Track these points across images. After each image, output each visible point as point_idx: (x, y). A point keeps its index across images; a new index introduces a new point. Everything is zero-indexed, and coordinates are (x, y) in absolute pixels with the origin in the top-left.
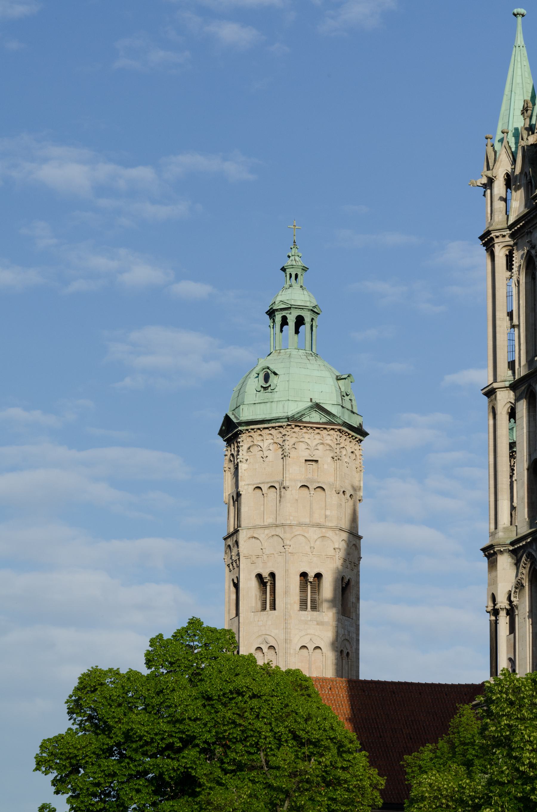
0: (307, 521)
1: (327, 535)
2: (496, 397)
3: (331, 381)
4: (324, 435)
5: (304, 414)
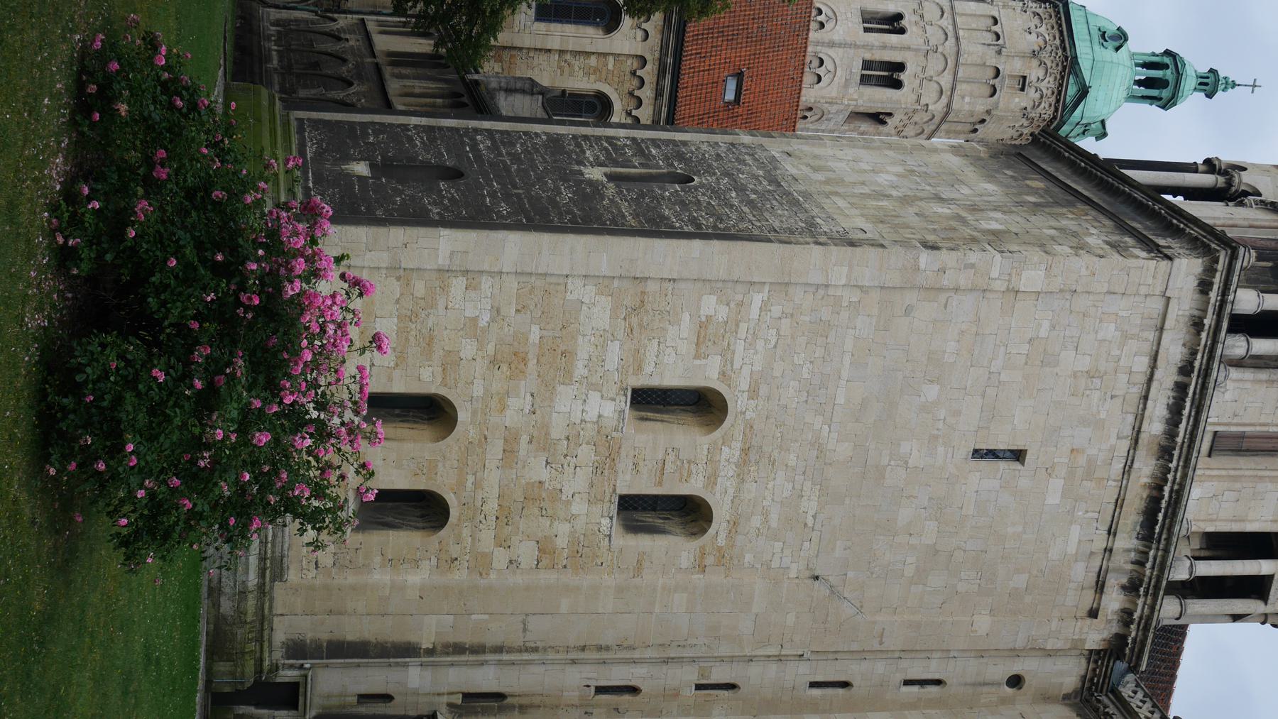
0: (960, 74)
1: (943, 97)
4: (1051, 100)
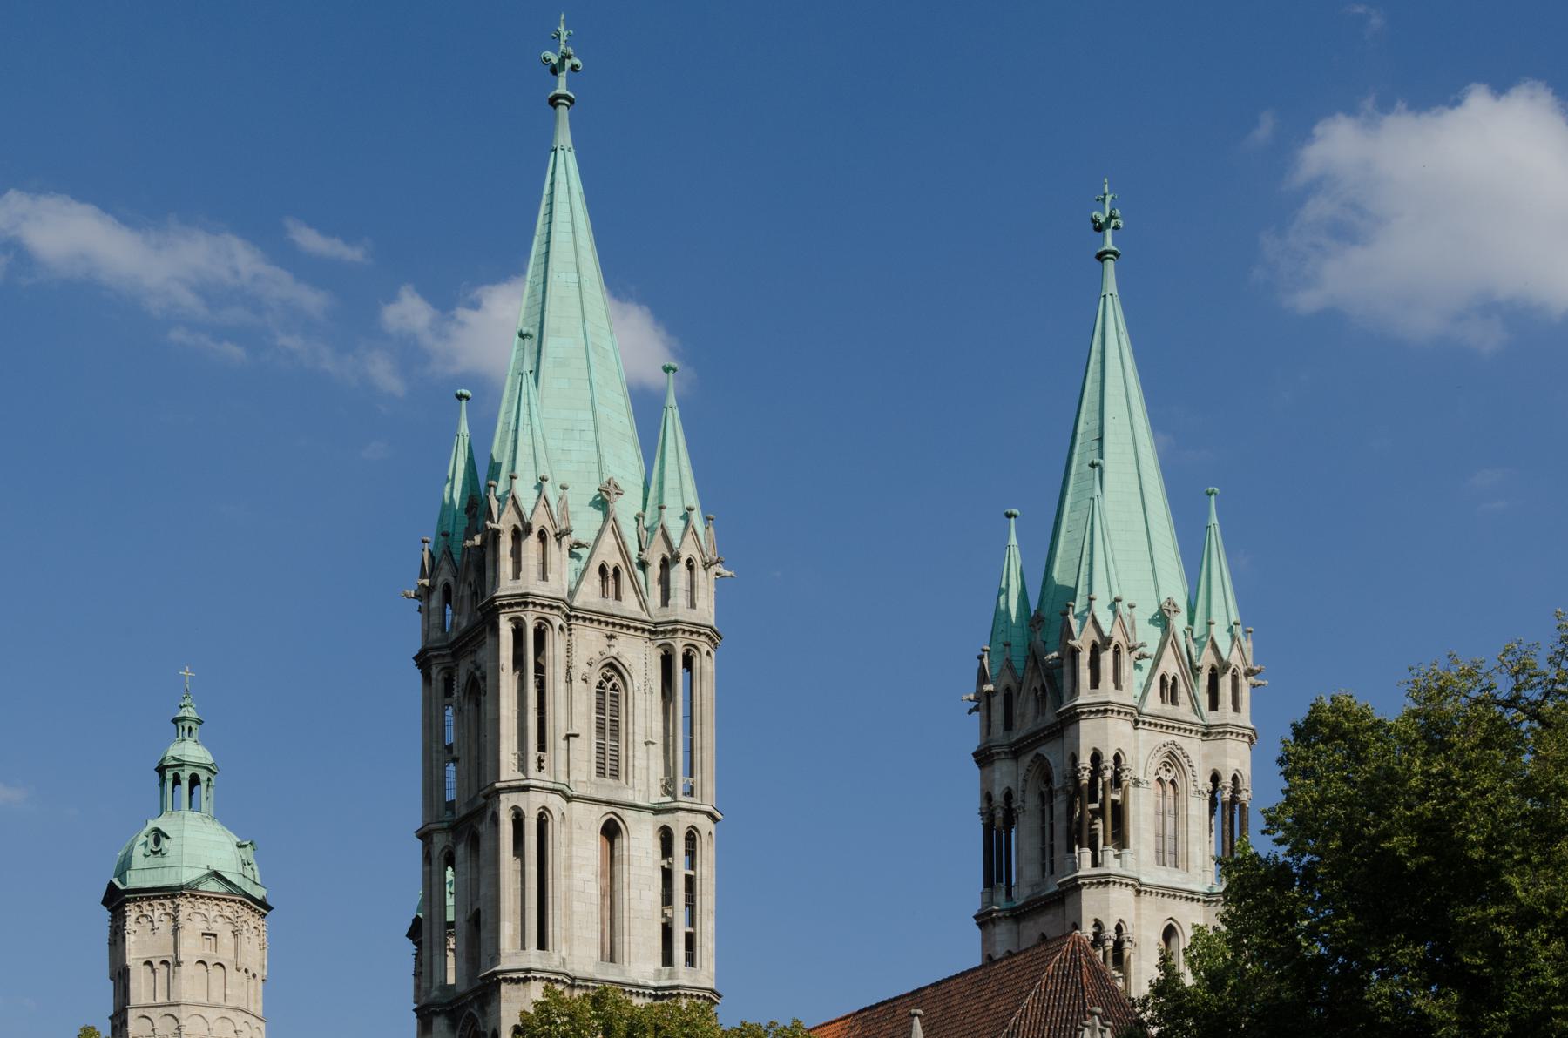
0: (204, 1000)
2: (432, 839)
3: (232, 848)
5: (200, 883)
